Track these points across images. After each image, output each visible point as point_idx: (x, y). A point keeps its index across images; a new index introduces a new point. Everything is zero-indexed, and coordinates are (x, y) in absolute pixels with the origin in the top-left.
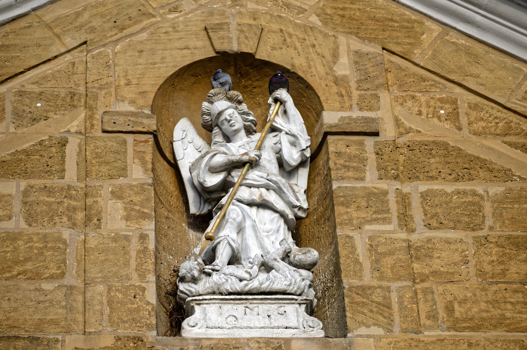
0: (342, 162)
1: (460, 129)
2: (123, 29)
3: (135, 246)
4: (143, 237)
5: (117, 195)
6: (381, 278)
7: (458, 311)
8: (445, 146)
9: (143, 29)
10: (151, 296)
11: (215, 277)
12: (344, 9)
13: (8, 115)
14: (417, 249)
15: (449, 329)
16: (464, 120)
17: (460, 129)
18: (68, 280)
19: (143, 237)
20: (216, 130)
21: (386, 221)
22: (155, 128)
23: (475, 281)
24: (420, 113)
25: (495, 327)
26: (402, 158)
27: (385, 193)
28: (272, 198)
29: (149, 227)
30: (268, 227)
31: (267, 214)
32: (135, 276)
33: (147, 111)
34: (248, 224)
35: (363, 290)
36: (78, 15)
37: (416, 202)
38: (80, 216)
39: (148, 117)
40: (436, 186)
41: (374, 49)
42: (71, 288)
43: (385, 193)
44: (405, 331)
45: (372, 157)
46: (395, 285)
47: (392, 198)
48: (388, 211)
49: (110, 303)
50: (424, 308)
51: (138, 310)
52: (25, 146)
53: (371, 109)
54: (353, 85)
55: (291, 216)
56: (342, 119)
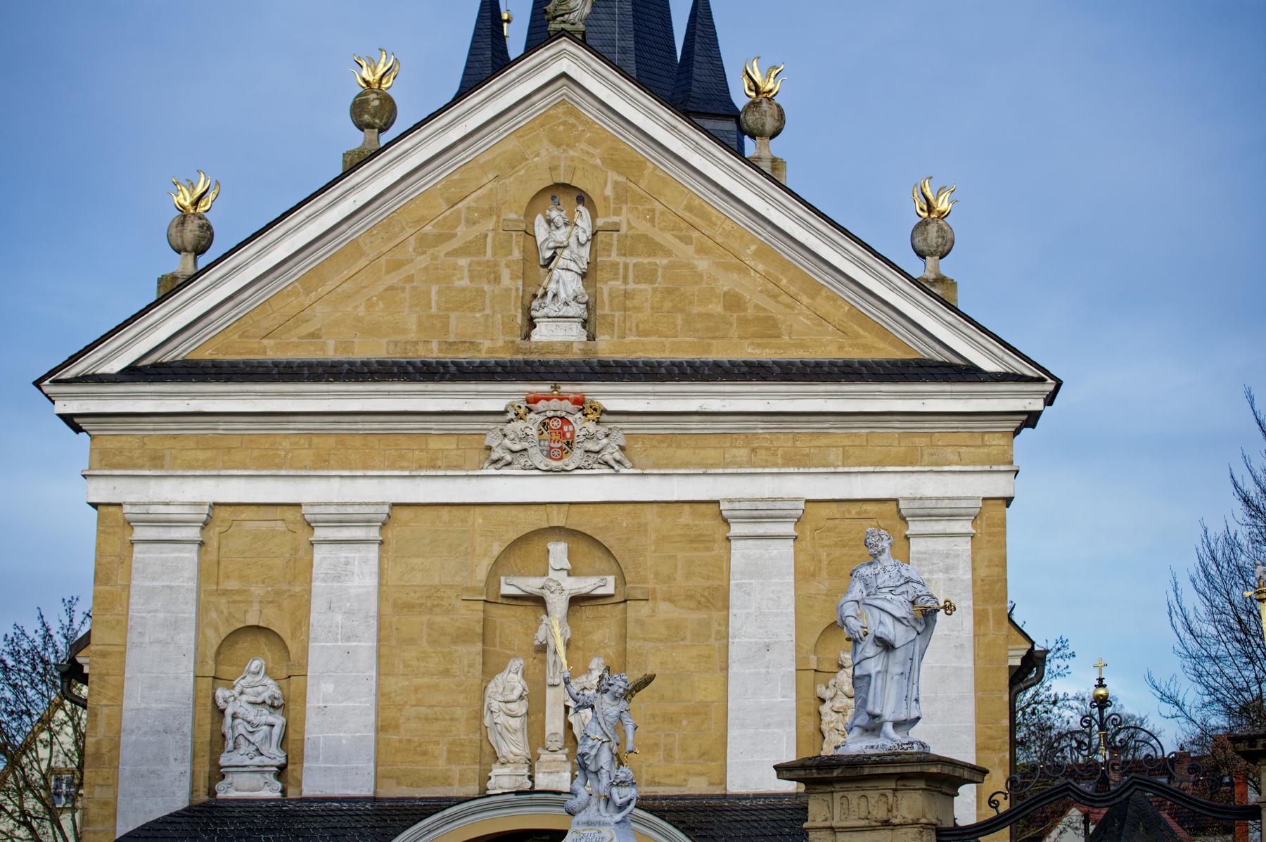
0: (602, 246)
1: (654, 226)
2: (514, 168)
3: (513, 294)
4: (517, 289)
5: (508, 266)
6: (612, 310)
7: (641, 327)
8: (646, 236)
9: (523, 167)
10: (519, 320)
11: (546, 310)
12: (612, 155)
13: (463, 221)
14: (629, 294)
15: (636, 336)
16: (657, 221)
17: (654, 226)
18: (487, 312)
19: (517, 289)
20: (552, 224)
21: (617, 279)
22: (524, 228)
23: (649, 311)
24: (638, 217)
25: (654, 335)
26: (628, 243)
27: (618, 264)
28: (572, 266)
29: (520, 283)
30: (569, 279)
31: (569, 273)
32: (513, 308)
33: (522, 218)
34: (561, 281)
35: (604, 317)
36: (494, 159)
37: (631, 268)
38: (492, 276)
39: (522, 222)
40: (640, 260)
41: (621, 179)
42: (488, 315)
43: (618, 264)
44: (619, 337)
45: (615, 243)
46: (617, 314)
47: (621, 266)
48: (618, 274)
49: (503, 324)
50: (628, 324)
51: (513, 327)
52: (470, 238)
53: (618, 216)
54: (612, 201)
55: (579, 272)
56: (605, 223)
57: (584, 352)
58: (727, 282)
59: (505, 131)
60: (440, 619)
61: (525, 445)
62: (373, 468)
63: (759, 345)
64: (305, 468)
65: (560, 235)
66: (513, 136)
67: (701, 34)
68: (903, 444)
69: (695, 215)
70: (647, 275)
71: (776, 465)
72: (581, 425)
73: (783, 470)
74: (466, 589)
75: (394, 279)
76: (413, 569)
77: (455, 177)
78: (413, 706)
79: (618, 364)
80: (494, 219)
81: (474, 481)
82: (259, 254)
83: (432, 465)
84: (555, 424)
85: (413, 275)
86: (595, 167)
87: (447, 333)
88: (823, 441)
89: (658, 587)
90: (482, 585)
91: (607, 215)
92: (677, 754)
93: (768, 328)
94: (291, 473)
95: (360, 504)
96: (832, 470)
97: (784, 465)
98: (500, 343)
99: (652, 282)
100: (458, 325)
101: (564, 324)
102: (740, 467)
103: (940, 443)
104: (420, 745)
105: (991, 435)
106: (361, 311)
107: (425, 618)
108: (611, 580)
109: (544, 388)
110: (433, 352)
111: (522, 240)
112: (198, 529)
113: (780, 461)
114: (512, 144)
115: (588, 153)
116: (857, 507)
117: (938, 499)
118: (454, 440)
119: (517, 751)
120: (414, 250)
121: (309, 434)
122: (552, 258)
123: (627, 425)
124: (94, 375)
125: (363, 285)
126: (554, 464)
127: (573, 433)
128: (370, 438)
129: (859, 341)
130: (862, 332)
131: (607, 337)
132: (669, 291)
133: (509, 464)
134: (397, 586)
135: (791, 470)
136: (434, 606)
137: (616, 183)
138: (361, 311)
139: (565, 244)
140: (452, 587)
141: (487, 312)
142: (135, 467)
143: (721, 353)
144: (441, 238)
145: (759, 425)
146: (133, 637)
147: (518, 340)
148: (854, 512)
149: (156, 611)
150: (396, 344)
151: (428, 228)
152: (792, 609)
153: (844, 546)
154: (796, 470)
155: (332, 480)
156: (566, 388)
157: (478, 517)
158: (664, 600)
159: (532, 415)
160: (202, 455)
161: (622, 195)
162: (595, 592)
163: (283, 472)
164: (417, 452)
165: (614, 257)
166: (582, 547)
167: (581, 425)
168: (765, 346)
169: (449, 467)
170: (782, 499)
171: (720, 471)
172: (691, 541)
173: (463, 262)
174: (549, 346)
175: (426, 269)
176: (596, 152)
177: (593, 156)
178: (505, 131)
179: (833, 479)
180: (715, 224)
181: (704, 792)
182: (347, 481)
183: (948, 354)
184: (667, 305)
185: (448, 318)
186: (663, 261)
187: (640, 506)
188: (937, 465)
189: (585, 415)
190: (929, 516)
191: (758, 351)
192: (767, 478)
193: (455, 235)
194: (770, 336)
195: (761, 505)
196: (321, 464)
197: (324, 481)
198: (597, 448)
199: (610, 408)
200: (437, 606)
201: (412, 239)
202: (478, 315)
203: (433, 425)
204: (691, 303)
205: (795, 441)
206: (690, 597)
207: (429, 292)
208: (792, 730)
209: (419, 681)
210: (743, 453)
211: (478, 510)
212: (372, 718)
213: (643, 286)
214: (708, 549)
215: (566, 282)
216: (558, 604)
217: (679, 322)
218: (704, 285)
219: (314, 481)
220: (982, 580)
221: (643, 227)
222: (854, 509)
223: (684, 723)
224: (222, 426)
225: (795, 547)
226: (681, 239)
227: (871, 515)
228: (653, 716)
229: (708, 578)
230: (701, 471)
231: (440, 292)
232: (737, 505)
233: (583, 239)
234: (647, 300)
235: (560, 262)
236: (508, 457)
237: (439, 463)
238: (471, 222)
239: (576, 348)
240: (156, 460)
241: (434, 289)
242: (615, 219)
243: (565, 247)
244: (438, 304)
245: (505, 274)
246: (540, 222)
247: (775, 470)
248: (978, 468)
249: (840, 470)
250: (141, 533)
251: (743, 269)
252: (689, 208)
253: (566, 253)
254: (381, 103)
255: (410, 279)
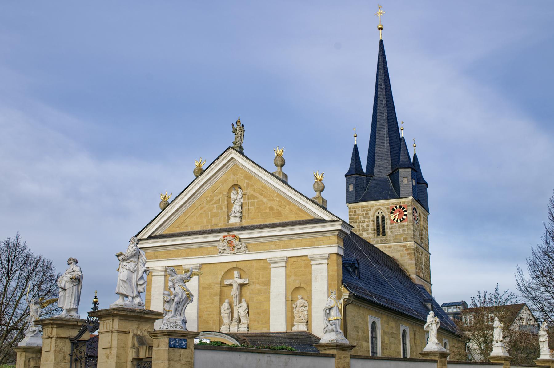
3: (225, 212)
8: (253, 195)
16: (255, 191)
18: (220, 217)
19: (226, 211)
21: (246, 206)
28: (238, 204)
29: (227, 209)
37: (250, 203)
38: (221, 208)
40: (251, 201)
41: (248, 181)
45: (246, 197)
57: (240, 224)
58: (270, 204)
59: (223, 173)
60: (211, 291)
61: (225, 248)
62: (197, 256)
63: (277, 219)
64: (184, 257)
65: (235, 197)
66: (225, 174)
67: (402, 148)
68: (310, 241)
69: (264, 188)
70: (253, 204)
71: (281, 249)
72: (235, 242)
73: (281, 250)
74: (216, 283)
75: (201, 211)
76: (206, 279)
77: (214, 186)
78: (206, 311)
79: (245, 227)
80: (221, 194)
81: (217, 257)
82: (172, 208)
83: (209, 254)
84: (230, 242)
85: (205, 210)
86: (242, 179)
87: (212, 223)
88: (291, 242)
89: (256, 281)
90: (220, 282)
91: (245, 191)
92: (260, 322)
93: (279, 214)
94: (181, 258)
95: (193, 264)
96: (293, 249)
97: (282, 249)
98: (223, 224)
99: (254, 206)
100: (215, 221)
101: (235, 218)
102: (273, 249)
103: (319, 240)
104: (207, 321)
105: (332, 237)
106: (195, 220)
107: (208, 291)
108: (247, 279)
109: (226, 234)
110: (209, 228)
111: (227, 199)
112: (164, 272)
113: (282, 248)
114: (225, 176)
115: (240, 176)
116: (301, 258)
117: (317, 255)
118: (213, 248)
119: (227, 322)
120: (206, 204)
121: (185, 249)
122: (234, 202)
123: (247, 241)
124: (142, 239)
125: (196, 213)
126: (231, 252)
127: (234, 244)
128: (197, 249)
129: (300, 215)
130: (300, 213)
131: (244, 220)
132: (257, 208)
133: (223, 253)
134: (203, 283)
135: (283, 250)
136: (210, 288)
137: (247, 183)
138: (195, 220)
139: (236, 199)
140: (213, 283)
141: (220, 217)
142: (153, 259)
143: (268, 222)
144: (211, 200)
145: (276, 239)
146: (152, 298)
147: (226, 223)
148: (300, 259)
149: (156, 291)
150: (202, 226)
151: (208, 198)
152: (284, 285)
153: (297, 268)
154: (284, 250)
155: (189, 259)
156: (231, 233)
157: (219, 265)
158: (257, 284)
159: (225, 241)
160: (165, 255)
161: (248, 185)
162: (244, 283)
163: (179, 258)
164: (206, 252)
165: (246, 201)
166: (242, 273)
167: (235, 242)
168: (279, 219)
169: (212, 255)
170: (281, 257)
171: (267, 251)
172: (263, 269)
173: (215, 206)
174: (232, 224)
175: (208, 208)
176: (242, 175)
177: (242, 177)
178: (223, 173)
179: (293, 251)
180: (267, 190)
181: (266, 332)
182: (192, 259)
183: (320, 217)
184: (257, 211)
185: (212, 219)
186: (256, 200)
187: (252, 261)
188: (318, 246)
189: (236, 240)
190: (316, 259)
191: (277, 220)
192: (279, 252)
193: (213, 200)
194: (280, 216)
195: (276, 259)
196: (188, 255)
197: (188, 259)
198: (239, 247)
199: (241, 237)
200: (210, 288)
201: (205, 202)
202: (218, 218)
203: (208, 245)
204: (262, 210)
205: (285, 242)
206: (263, 283)
207: (208, 214)
208: (285, 316)
209: (207, 306)
210: (273, 246)
211: (219, 264)
212: (196, 315)
213: (252, 207)
214: (267, 271)
215: (236, 207)
216: (235, 286)
217: (260, 215)
218: (265, 205)
219: (186, 259)
220: (331, 275)
221: (252, 193)
222: (300, 258)
223: (262, 314)
224: (168, 248)
225: (285, 269)
226: (260, 194)
227: (304, 260)
228: (255, 313)
229: (267, 278)
230: (263, 252)
231: (211, 213)
232: (271, 259)
233: (240, 197)
234: (253, 210)
235: (235, 203)
236: (222, 251)
237: (210, 254)
238: (217, 196)
239: (238, 224)
240: (157, 257)
241: (209, 213)
242: (246, 191)
243: (236, 200)
244: (210, 216)
245: (224, 207)
246: (232, 194)
247: (280, 250)
248: (330, 246)
249: (294, 249)
250: (154, 274)
251: (274, 200)
252: (262, 187)
253: (236, 201)
254: (198, 170)
255: (205, 211)
